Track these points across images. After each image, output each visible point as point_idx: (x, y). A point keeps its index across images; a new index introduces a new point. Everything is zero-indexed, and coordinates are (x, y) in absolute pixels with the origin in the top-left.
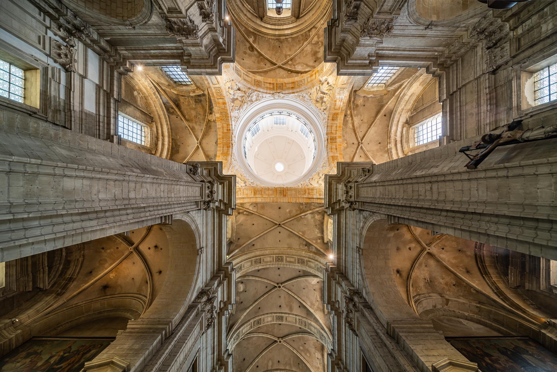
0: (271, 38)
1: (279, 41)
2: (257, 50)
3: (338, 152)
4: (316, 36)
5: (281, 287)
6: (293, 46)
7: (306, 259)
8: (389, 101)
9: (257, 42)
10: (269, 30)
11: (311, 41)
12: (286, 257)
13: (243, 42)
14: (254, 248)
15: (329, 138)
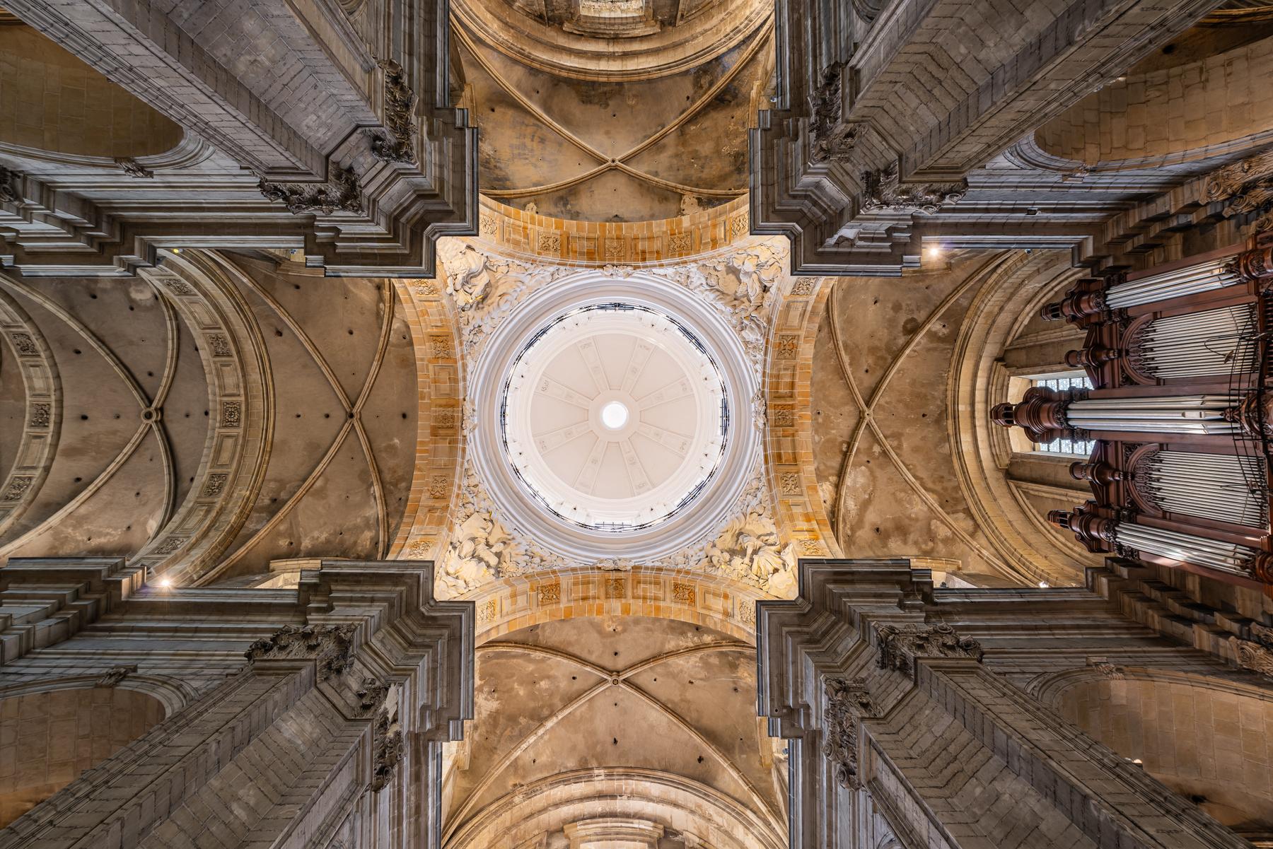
0: (949, 387)
1: (940, 414)
2: (907, 344)
3: (572, 604)
4: (949, 533)
5: (149, 422)
7: (219, 501)
8: (738, 771)
9: (934, 345)
10: (969, 383)
11: (937, 518)
12: (236, 437)
13: (927, 300)
15: (622, 575)
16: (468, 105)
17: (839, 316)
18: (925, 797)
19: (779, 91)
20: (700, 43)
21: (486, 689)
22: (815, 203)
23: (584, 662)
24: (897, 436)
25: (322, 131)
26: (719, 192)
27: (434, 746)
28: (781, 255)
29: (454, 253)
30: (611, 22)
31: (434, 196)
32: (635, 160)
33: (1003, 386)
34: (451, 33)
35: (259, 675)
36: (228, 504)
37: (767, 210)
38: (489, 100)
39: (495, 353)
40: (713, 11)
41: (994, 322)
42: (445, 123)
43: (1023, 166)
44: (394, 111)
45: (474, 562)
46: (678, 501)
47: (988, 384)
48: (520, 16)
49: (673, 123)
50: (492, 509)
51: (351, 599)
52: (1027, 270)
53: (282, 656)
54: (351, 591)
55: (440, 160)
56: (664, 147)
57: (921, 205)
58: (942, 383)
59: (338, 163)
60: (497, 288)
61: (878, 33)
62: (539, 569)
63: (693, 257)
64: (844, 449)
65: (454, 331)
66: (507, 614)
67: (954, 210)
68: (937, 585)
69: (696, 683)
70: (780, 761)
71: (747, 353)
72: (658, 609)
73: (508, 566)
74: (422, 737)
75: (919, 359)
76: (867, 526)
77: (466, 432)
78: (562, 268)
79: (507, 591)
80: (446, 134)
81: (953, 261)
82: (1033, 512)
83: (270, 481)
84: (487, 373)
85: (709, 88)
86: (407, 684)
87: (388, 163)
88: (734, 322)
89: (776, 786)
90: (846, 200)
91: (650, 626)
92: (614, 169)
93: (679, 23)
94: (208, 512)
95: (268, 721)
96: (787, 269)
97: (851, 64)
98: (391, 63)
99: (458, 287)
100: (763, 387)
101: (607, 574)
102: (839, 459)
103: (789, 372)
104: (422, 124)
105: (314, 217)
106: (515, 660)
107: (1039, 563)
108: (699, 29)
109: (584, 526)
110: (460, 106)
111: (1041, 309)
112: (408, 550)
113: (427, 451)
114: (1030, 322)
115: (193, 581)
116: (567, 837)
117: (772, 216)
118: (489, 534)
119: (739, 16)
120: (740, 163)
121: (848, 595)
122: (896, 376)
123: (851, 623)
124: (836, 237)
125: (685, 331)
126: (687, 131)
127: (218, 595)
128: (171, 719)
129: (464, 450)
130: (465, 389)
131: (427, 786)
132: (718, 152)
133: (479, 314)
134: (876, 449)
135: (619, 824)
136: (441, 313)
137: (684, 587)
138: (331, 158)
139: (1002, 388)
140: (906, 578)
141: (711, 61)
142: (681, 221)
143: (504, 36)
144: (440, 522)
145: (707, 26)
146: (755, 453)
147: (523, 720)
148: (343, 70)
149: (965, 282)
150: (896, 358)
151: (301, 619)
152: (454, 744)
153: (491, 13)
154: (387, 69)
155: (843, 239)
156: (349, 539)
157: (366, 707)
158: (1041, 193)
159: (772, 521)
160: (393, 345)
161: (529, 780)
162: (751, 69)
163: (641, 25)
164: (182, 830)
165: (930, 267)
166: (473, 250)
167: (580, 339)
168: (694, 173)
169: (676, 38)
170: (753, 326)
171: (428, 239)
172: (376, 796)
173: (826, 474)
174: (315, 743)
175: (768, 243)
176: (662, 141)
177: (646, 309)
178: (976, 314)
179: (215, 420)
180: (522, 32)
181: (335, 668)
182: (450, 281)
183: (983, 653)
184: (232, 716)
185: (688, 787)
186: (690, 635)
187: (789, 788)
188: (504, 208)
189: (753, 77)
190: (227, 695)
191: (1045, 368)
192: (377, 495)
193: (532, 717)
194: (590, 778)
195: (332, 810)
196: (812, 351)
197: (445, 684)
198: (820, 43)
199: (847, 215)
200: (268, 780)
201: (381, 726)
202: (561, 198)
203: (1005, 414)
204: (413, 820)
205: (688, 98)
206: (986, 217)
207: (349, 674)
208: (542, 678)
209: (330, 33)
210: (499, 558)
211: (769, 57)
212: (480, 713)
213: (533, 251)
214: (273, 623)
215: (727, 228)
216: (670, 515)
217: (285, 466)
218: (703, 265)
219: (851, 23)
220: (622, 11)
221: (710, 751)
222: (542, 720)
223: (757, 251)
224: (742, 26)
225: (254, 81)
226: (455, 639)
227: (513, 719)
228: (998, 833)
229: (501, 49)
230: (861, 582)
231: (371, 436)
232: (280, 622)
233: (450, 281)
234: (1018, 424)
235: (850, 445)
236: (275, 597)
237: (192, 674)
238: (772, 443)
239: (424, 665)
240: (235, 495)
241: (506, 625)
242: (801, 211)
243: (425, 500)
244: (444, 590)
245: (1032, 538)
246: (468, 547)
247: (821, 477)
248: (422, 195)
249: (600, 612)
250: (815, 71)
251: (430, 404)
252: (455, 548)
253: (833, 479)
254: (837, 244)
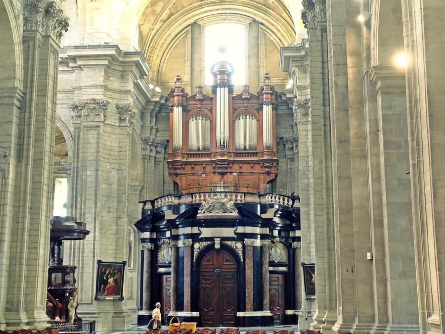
114: (271, 40)
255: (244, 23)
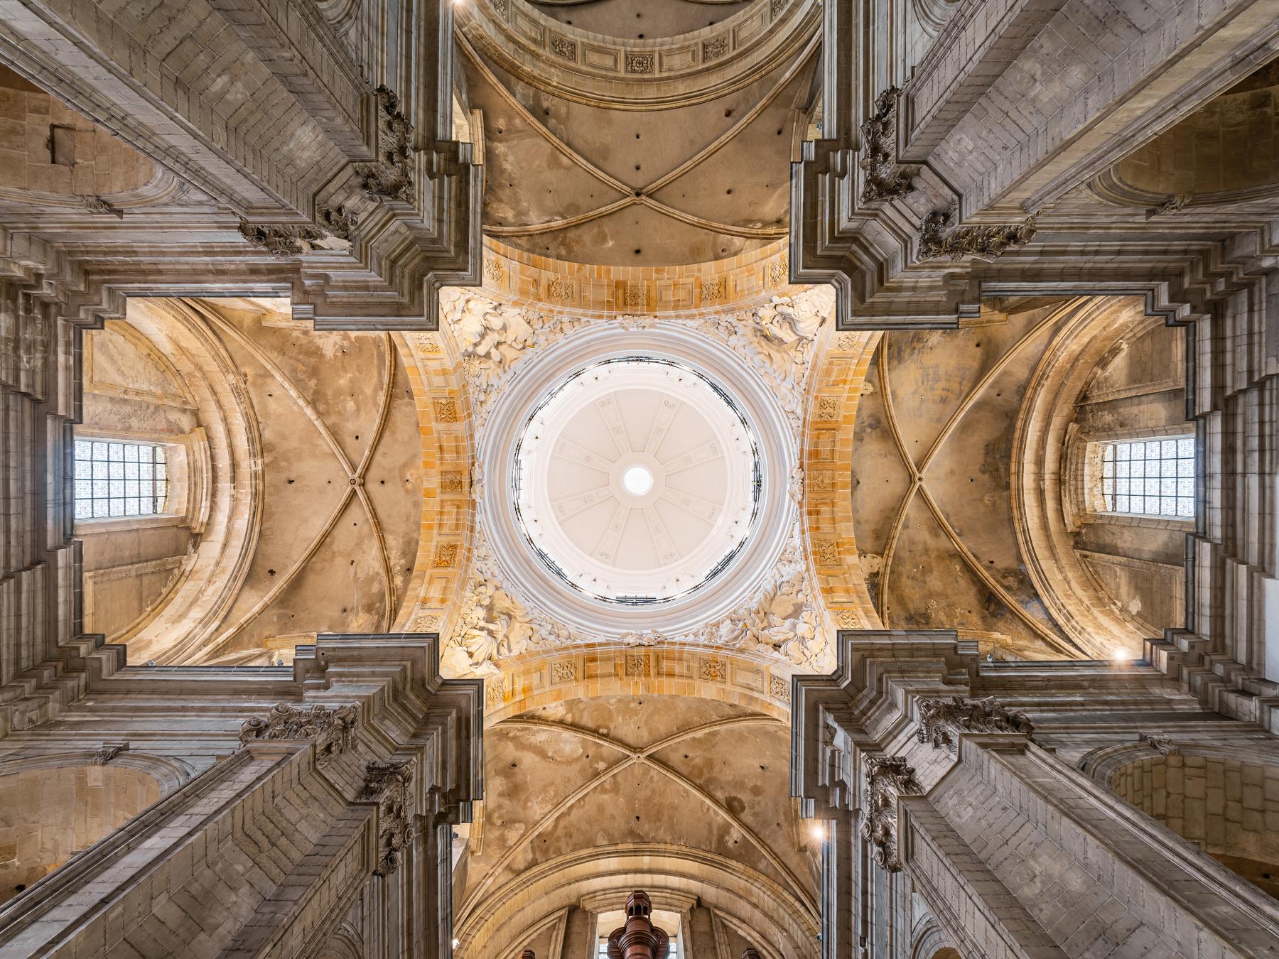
0: (669, 847)
1: (639, 836)
2: (716, 802)
3: (435, 435)
4: (510, 843)
6: (590, 822)
7: (546, 53)
9: (715, 831)
10: (674, 868)
11: (526, 831)
12: (615, 69)
13: (765, 824)
14: (728, 102)
15: (466, 488)
16: (983, 318)
17: (747, 727)
18: (233, 811)
19: (1000, 664)
20: (1054, 577)
21: (346, 343)
22: (873, 702)
23: (374, 448)
24: (616, 788)
25: (955, 156)
26: (886, 596)
27: (287, 289)
28: (815, 664)
29: (817, 303)
30: (1079, 477)
31: (881, 282)
32: (921, 503)
33: (671, 905)
34: (1067, 298)
35: (362, 101)
36: (543, 62)
37: (865, 650)
38: (989, 341)
39: (707, 350)
40: (1091, 591)
41: (741, 897)
42: (963, 292)
43: (915, 934)
44: (977, 236)
45: (480, 329)
46: (545, 551)
47: (672, 889)
48: (1086, 375)
49: (964, 546)
50: (538, 349)
51: (441, 198)
52: (798, 935)
53: (382, 125)
54: (450, 198)
55: (922, 287)
56: (937, 536)
57: (871, 820)
58: (673, 839)
59: (918, 174)
60: (778, 351)
61: (1066, 776)
62: (473, 400)
63: (812, 567)
64: (601, 731)
65: (731, 305)
66: (425, 366)
67: (865, 856)
68: (456, 828)
69: (352, 568)
70: (270, 657)
71: (706, 625)
72: (430, 527)
73: (476, 366)
74: (295, 276)
75: (700, 814)
76: (518, 754)
77: (620, 319)
78: (800, 423)
79: (449, 365)
80: (950, 294)
81: (808, 853)
82: (533, 934)
83: (568, 107)
84: (684, 341)
85: (1002, 586)
86: (352, 259)
87: (919, 230)
88: (741, 612)
89: (244, 653)
90: (877, 737)
91: (412, 519)
92: (911, 480)
93: (1078, 553)
94: (535, 41)
95: (314, 112)
96: (800, 671)
97: (1030, 744)
98: (1032, 231)
99: (779, 309)
100: (669, 643)
101: (467, 472)
102: (590, 724)
103: (685, 671)
104: (962, 267)
105: (857, 149)
106: (376, 374)
107: (479, 939)
108: (1070, 575)
109: (518, 448)
110: (983, 309)
111: (754, 949)
112: (493, 258)
113: (599, 276)
114: (741, 937)
115: (460, 27)
116: (192, 431)
117: (859, 655)
118: (510, 346)
119: (1086, 620)
120: (919, 620)
121: (444, 732)
122: (681, 788)
123: (415, 736)
124: (836, 725)
125: (731, 557)
126: (954, 561)
127: (445, 55)
128: (316, 8)
129: (600, 317)
130: (667, 318)
131: (245, 282)
132: (931, 595)
133: (749, 332)
134: (601, 766)
135: (205, 486)
136: (751, 291)
137: (453, 555)
138: (924, 167)
139: (667, 904)
140: (463, 795)
141: (1034, 589)
142: (853, 554)
143: (1063, 356)
144: (523, 292)
145: (1074, 584)
146: (597, 633)
147: (313, 383)
148: (1024, 178)
149: (785, 867)
150: (700, 788)
151: (420, 145)
152: (288, 310)
153: (1089, 342)
154: (1025, 228)
155: (833, 733)
156: (505, 194)
157: (327, 216)
158: (885, 952)
159: (524, 651)
160: (715, 239)
161: (251, 390)
162: (1024, 632)
163: (1075, 510)
164: (201, 23)
165: (802, 829)
166: (821, 325)
167: (722, 442)
168: (907, 568)
169: (1060, 550)
170: (736, 633)
171: (833, 275)
172: (234, 228)
173: (574, 710)
174: (290, 162)
175: (828, 650)
176: (942, 534)
177: (754, 515)
178: (749, 877)
179: (634, 45)
180: (1067, 376)
181: (368, 181)
182: (786, 299)
183: (383, 876)
184: (319, 74)
185: (244, 559)
186: (403, 561)
187: (241, 666)
188: (866, 360)
189: (1016, 635)
190: (341, 67)
191: (690, 952)
192: (552, 224)
193: (316, 392)
194: (252, 455)
195: (221, 182)
196: (708, 697)
197: (351, 300)
198: (1054, 711)
199: (859, 737)
200: (252, 112)
201: (308, 233)
202: (879, 422)
203: (639, 907)
204: (210, 267)
205: (992, 562)
206: (857, 891)
207: (363, 197)
208: (357, 404)
209: (1066, 162)
210: (485, 356)
211: (1039, 652)
212: (320, 337)
213: (820, 391)
214: (416, 114)
215: (845, 605)
216: (530, 541)
217: (583, 123)
218: (803, 578)
219: (1078, 745)
220: (1091, 489)
221: (280, 582)
222: (313, 403)
223: (819, 638)
224: (1073, 623)
225: (1013, 80)
226: (398, 310)
227: (314, 372)
228: (195, 888)
229: (1048, 353)
230: (459, 747)
231: (616, 217)
232: (417, 122)
233: (786, 299)
234: (629, 921)
235: (605, 737)
236: (444, 116)
237: (363, 28)
238: (608, 652)
239: (372, 277)
240: (553, 70)
241: (413, 364)
242: (865, 687)
243: (547, 276)
244: (450, 297)
245: (506, 933)
246: (496, 323)
247: (572, 704)
248: (882, 268)
249: (427, 465)
250: (1022, 704)
251: (650, 280)
252: (495, 308)
253: (569, 719)
254: (827, 726)
255: (679, 910)
